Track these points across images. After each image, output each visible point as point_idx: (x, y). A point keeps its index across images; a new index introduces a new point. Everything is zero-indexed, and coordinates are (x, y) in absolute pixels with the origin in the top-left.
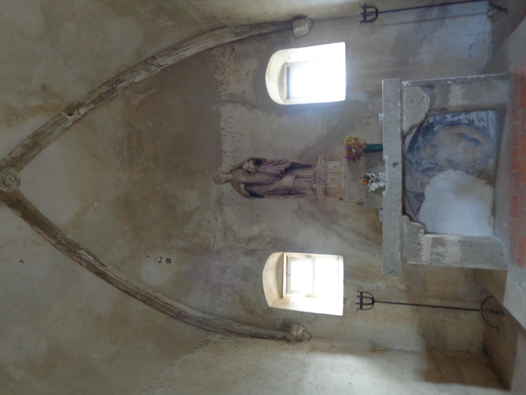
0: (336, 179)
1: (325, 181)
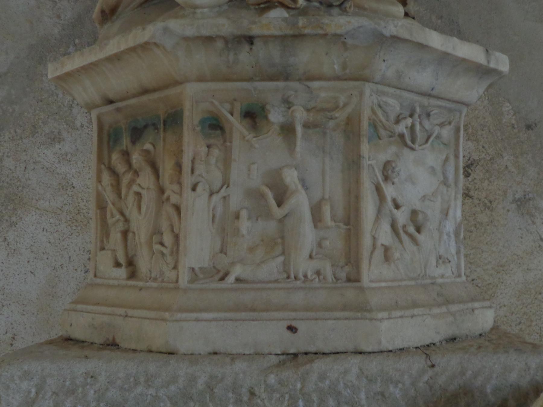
0: (280, 242)
1: (254, 116)
